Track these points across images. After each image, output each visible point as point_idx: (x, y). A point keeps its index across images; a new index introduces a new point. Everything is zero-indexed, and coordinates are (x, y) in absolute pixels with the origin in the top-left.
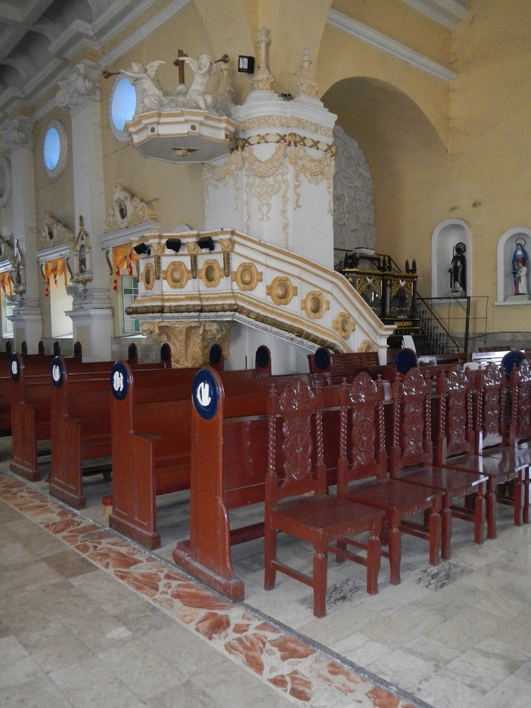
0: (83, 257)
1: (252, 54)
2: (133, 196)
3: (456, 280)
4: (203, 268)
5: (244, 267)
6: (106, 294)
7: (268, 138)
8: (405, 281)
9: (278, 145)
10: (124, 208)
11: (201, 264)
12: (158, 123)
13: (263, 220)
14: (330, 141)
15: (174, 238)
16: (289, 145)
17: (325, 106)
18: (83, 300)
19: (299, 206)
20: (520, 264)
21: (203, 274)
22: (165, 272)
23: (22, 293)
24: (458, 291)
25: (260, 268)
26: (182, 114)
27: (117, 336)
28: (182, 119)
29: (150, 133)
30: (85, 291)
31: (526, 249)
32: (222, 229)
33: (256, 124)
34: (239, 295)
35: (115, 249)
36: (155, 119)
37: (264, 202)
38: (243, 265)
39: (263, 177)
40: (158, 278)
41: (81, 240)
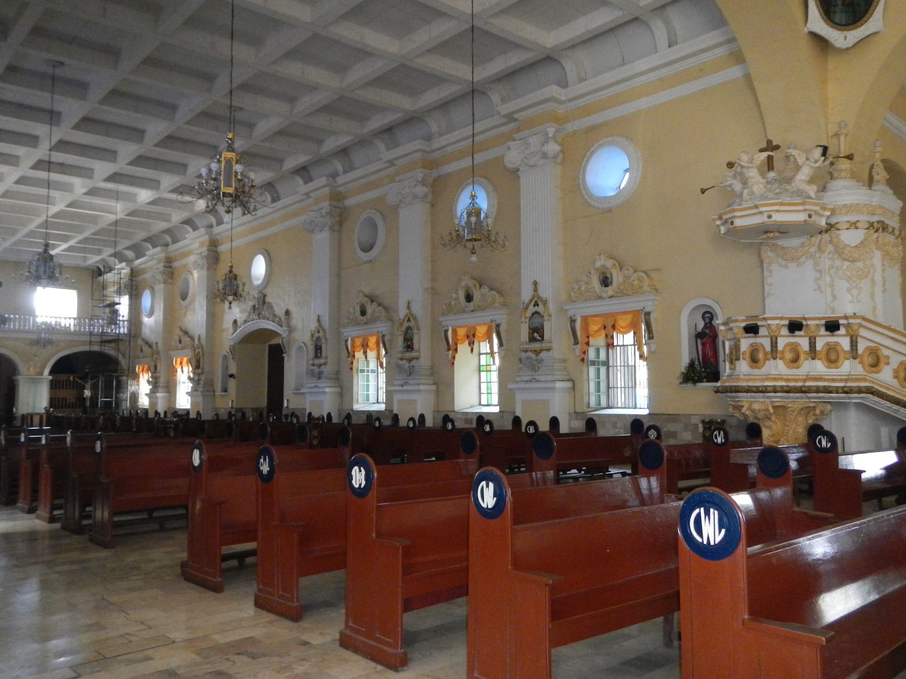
0: (536, 325)
5: (870, 350)
6: (562, 365)
7: (858, 225)
9: (866, 231)
10: (609, 276)
11: (820, 344)
12: (778, 211)
13: (853, 303)
15: (793, 319)
16: (877, 231)
18: (536, 371)
21: (823, 355)
22: (783, 352)
25: (886, 352)
26: (803, 204)
27: (578, 411)
28: (801, 208)
29: (766, 219)
34: (867, 378)
35: (585, 319)
37: (854, 285)
38: (868, 348)
39: (854, 261)
41: (534, 306)
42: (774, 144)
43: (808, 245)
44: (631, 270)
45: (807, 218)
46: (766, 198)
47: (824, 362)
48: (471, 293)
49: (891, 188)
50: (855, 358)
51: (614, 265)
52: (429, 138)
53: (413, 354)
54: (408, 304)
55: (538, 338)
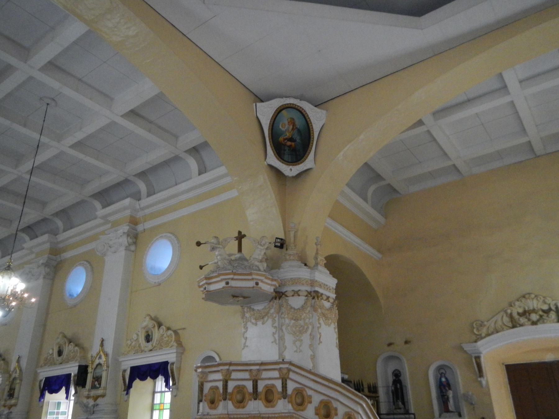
0: (98, 375)
1: (283, 237)
2: (160, 325)
3: (397, 398)
4: (263, 391)
7: (300, 293)
8: (372, 401)
9: (307, 297)
10: (150, 334)
12: (232, 279)
13: (297, 352)
14: (333, 296)
16: (314, 298)
17: (330, 273)
19: (321, 342)
20: (447, 388)
21: (263, 396)
22: (232, 394)
23: (10, 407)
24: (400, 409)
25: (310, 392)
26: (250, 274)
28: (250, 277)
30: (94, 406)
31: (447, 376)
32: (283, 360)
33: (291, 283)
34: (294, 415)
36: (231, 276)
37: (297, 338)
38: (295, 389)
40: (225, 399)
42: (243, 234)
43: (268, 308)
45: (255, 285)
46: (226, 270)
47: (264, 402)
48: (61, 348)
49: (328, 269)
50: (285, 398)
52: (54, 233)
53: (13, 401)
54: (19, 358)
55: (98, 386)
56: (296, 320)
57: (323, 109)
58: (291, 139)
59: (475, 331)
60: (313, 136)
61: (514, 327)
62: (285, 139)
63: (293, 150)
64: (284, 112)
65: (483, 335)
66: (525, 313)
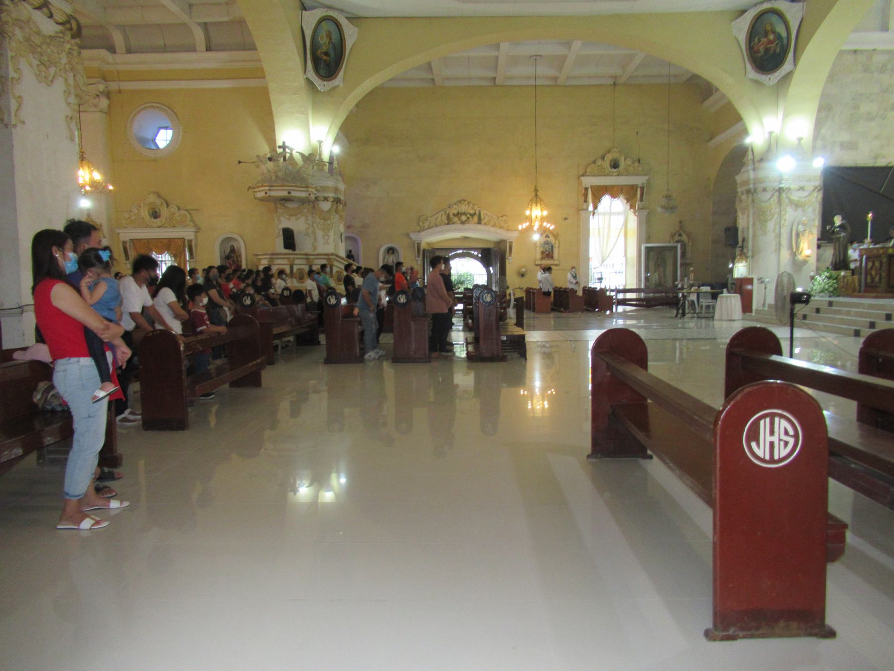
10: (157, 211)
12: (294, 190)
28: (305, 189)
38: (337, 272)
44: (176, 208)
50: (332, 277)
51: (162, 203)
56: (325, 220)
57: (357, 26)
58: (327, 54)
59: (421, 224)
60: (345, 53)
61: (448, 224)
62: (322, 53)
63: (328, 65)
64: (323, 23)
65: (426, 227)
66: (458, 215)
